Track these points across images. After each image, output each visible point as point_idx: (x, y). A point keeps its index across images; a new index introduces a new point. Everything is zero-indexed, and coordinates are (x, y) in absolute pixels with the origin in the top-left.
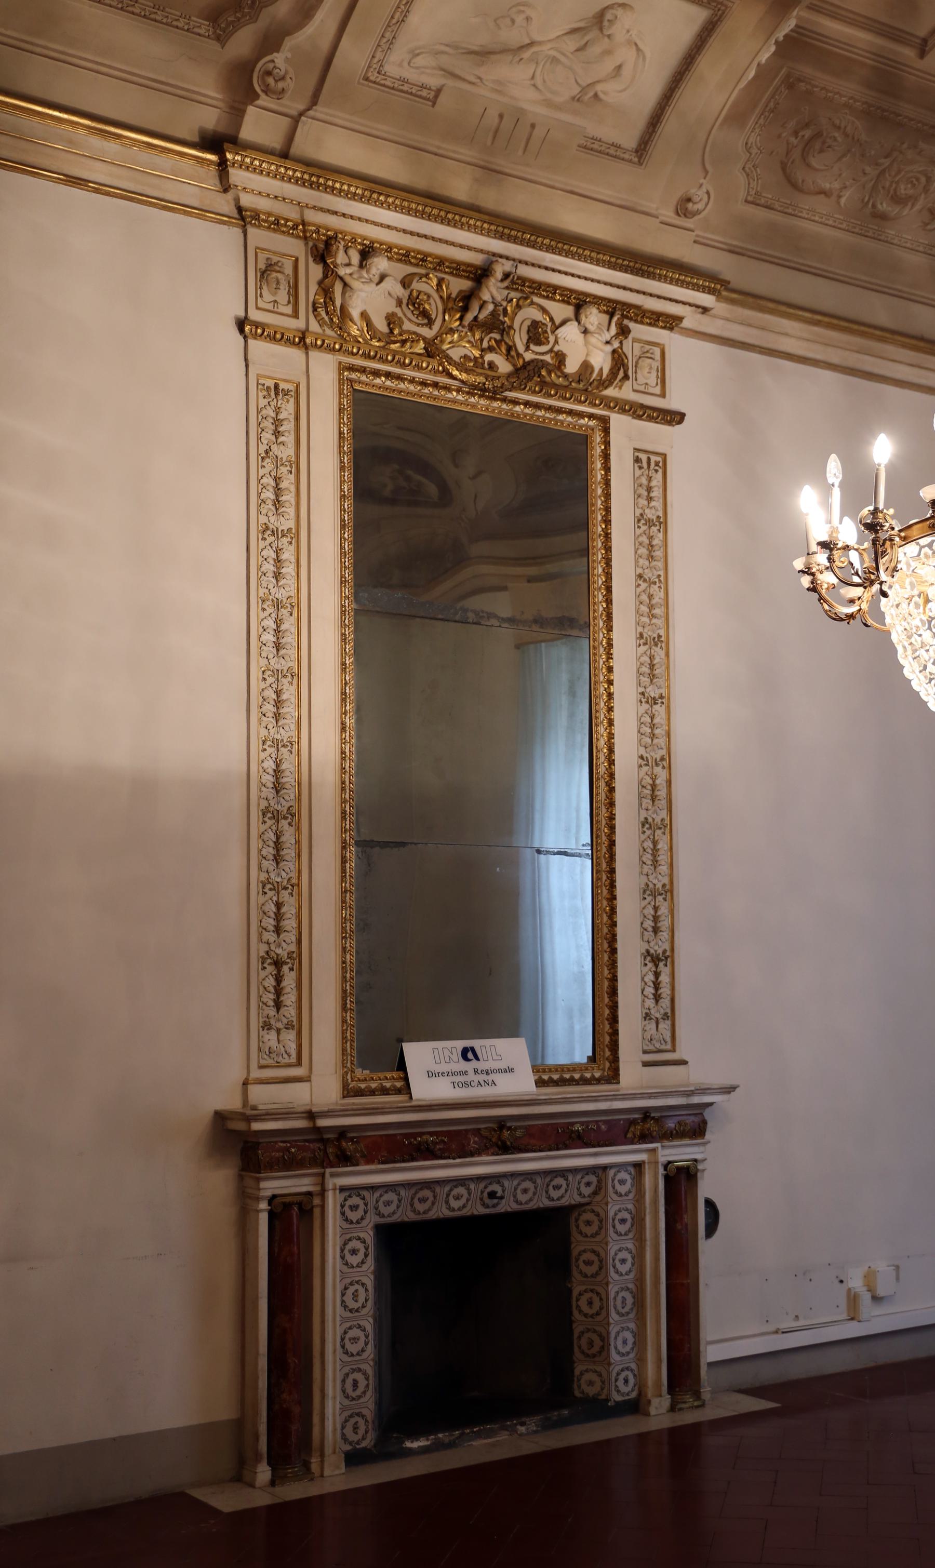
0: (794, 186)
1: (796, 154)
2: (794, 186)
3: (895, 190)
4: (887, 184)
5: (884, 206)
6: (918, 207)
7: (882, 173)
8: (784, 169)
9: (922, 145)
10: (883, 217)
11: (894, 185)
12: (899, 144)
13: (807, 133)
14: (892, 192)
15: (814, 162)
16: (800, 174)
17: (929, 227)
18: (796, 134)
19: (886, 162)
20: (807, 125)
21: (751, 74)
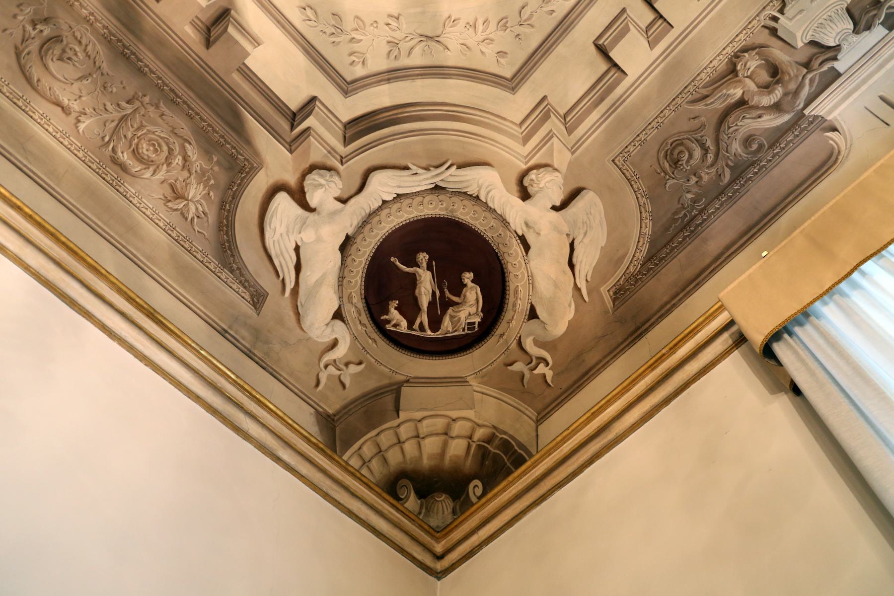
0: (29, 80)
1: (34, 46)
2: (29, 80)
3: (137, 145)
4: (130, 135)
5: (125, 157)
6: (160, 176)
7: (124, 119)
8: (18, 55)
9: (163, 108)
10: (123, 168)
11: (136, 140)
12: (140, 94)
14: (133, 146)
15: (52, 66)
16: (36, 72)
17: (170, 204)
18: (34, 24)
19: (129, 109)
20: (46, 21)
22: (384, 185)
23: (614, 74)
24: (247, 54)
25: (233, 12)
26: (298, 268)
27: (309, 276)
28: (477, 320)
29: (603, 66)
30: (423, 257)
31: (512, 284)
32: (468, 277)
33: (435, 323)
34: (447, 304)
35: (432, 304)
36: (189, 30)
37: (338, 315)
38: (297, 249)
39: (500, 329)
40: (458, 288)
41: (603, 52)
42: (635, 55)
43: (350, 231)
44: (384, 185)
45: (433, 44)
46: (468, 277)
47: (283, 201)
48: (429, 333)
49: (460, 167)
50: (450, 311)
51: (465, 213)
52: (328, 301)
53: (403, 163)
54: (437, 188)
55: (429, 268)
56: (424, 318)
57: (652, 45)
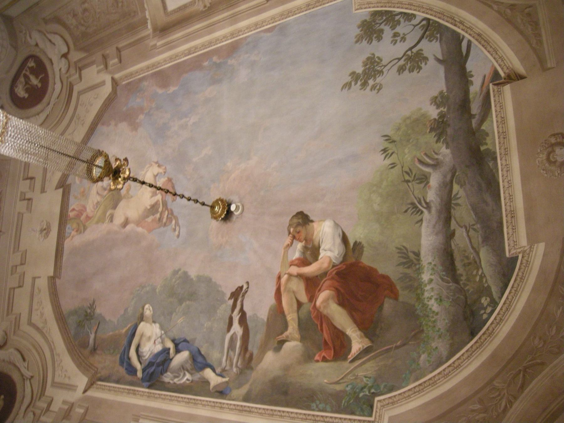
13: (120, 5)
21: (146, 6)
22: (58, 86)
23: (26, 176)
24: (97, 66)
25: (105, 71)
26: (50, 41)
27: (48, 44)
28: (16, 90)
29: (30, 175)
30: (39, 85)
31: (14, 107)
32: (26, 96)
33: (26, 77)
34: (27, 83)
35: (29, 79)
36: (108, 52)
37: (37, 45)
38: (54, 44)
39: (8, 95)
40: (27, 90)
41: (32, 178)
42: (24, 186)
43: (54, 66)
44: (58, 86)
46: (26, 96)
47: (65, 50)
48: (24, 72)
49: (48, 115)
50: (24, 83)
51: (39, 107)
52: (41, 45)
53: (59, 98)
54: (49, 104)
55: (37, 86)
56: (28, 73)
57: (21, 193)
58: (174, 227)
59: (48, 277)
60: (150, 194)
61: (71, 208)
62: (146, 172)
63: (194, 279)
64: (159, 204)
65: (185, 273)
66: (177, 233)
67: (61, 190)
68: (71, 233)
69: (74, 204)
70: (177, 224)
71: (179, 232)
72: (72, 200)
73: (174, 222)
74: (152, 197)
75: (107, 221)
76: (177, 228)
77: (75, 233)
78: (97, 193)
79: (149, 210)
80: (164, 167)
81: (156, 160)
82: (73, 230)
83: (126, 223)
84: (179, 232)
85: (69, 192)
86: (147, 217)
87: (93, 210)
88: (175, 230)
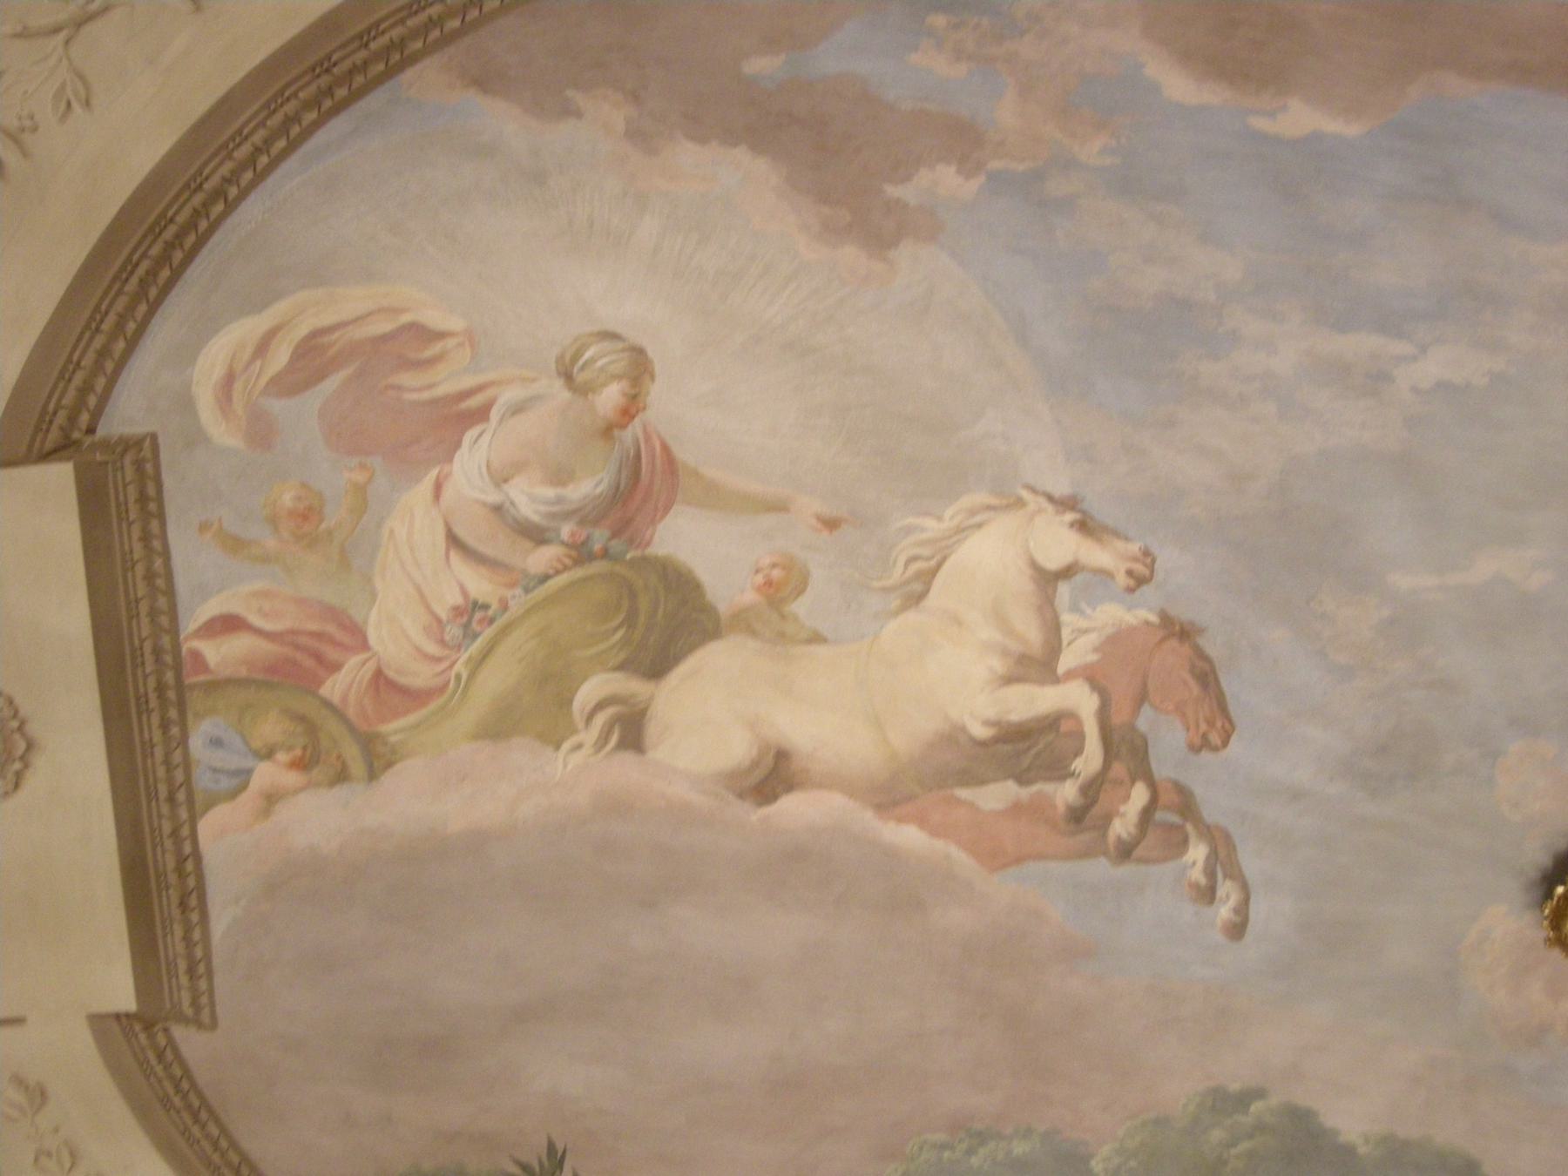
45: (62, 16)
58: (1197, 875)
59: (99, 1023)
60: (998, 665)
61: (195, 614)
62: (961, 531)
63: (1362, 1150)
64: (1080, 736)
65: (1300, 1121)
66: (1224, 912)
67: (60, 476)
68: (248, 772)
69: (223, 594)
70: (1223, 859)
71: (1243, 909)
72: (191, 557)
73: (1197, 852)
74: (1009, 680)
75: (590, 736)
76: (1226, 888)
77: (292, 778)
78: (453, 540)
79: (983, 744)
80: (1134, 548)
81: (1061, 489)
82: (268, 754)
83: (773, 775)
84: (1243, 909)
85: (151, 504)
86: (970, 778)
87: (432, 648)
88: (1208, 894)
